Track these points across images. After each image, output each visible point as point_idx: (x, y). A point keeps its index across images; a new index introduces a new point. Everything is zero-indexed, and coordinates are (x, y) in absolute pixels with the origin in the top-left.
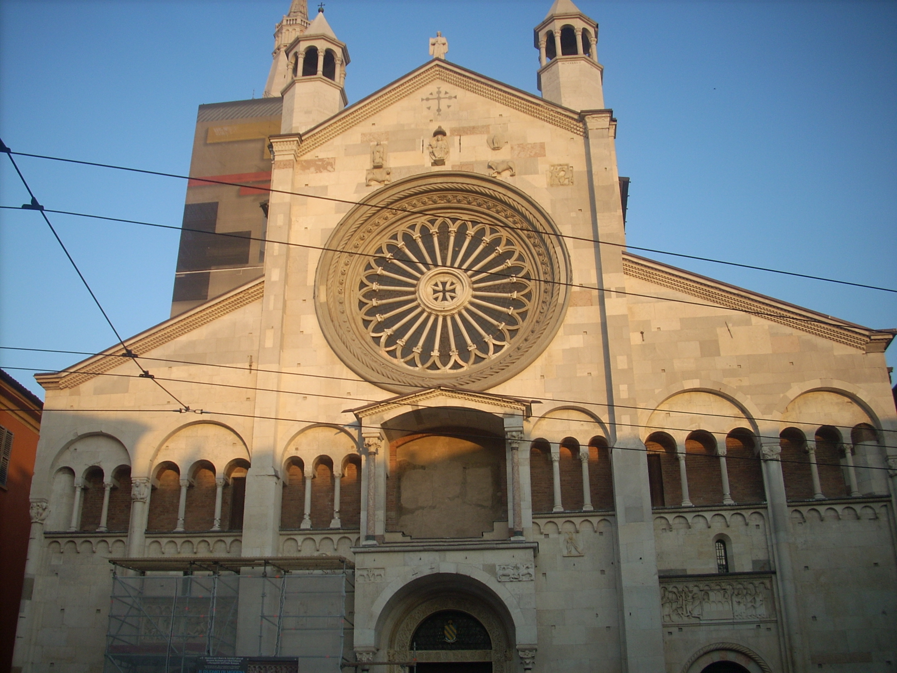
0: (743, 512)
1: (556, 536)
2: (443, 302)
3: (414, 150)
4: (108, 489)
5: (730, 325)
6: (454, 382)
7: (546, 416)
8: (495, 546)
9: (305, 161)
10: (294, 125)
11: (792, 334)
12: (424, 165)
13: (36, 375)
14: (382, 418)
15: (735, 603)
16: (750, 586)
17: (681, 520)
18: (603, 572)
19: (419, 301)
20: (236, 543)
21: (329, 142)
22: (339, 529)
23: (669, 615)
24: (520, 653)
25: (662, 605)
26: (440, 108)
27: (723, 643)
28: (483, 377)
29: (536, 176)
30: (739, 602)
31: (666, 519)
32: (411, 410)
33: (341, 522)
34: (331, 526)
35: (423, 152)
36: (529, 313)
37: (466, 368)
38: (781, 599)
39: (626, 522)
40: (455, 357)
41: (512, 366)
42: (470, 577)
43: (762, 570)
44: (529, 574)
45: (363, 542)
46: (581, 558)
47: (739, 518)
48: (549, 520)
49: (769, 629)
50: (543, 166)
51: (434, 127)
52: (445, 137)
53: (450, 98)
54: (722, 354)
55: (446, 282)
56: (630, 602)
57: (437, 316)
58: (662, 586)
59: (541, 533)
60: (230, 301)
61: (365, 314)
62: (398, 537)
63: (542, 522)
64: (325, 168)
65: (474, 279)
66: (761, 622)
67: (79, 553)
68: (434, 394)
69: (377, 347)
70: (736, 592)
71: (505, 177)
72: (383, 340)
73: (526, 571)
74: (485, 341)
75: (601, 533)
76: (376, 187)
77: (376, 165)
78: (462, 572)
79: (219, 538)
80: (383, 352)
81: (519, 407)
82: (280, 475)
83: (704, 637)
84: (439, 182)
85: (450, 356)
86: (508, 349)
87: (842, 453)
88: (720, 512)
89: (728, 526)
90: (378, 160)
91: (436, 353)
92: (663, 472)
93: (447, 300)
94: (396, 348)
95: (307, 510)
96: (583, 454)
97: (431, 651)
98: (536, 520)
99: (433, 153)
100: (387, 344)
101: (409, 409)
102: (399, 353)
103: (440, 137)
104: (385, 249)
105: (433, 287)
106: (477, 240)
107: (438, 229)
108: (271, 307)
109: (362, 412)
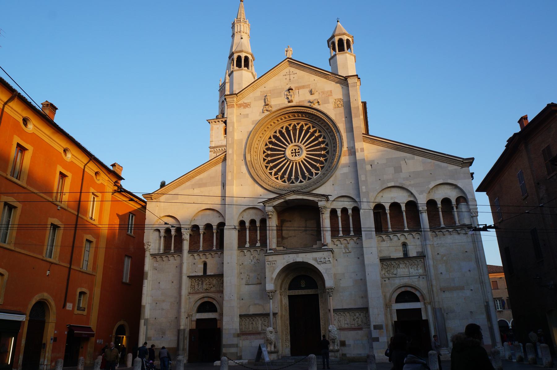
0: (412, 233)
1: (340, 245)
3: (281, 97)
4: (173, 236)
5: (406, 160)
7: (335, 200)
8: (316, 250)
9: (239, 104)
10: (234, 90)
11: (431, 162)
13: (143, 195)
14: (273, 205)
15: (409, 268)
16: (416, 262)
17: (388, 237)
18: (358, 258)
19: (286, 157)
20: (222, 254)
21: (248, 96)
22: (259, 246)
23: (384, 274)
24: (327, 290)
25: (382, 270)
26: (291, 78)
27: (405, 284)
29: (328, 104)
30: (411, 268)
31: (382, 237)
33: (261, 244)
34: (257, 245)
36: (328, 159)
37: (305, 182)
38: (428, 266)
39: (366, 239)
41: (321, 181)
42: (307, 263)
43: (421, 255)
44: (329, 260)
45: (268, 252)
46: (350, 253)
47: (411, 236)
48: (338, 239)
49: (423, 278)
50: (332, 100)
51: (288, 88)
52: (293, 91)
53: (294, 74)
54: (403, 172)
55: (296, 149)
56: (368, 270)
57: (293, 163)
58: (381, 263)
59: (335, 245)
61: (266, 163)
62: (282, 248)
63: (335, 240)
64: (247, 107)
65: (307, 147)
66: (420, 275)
67: (164, 261)
68: (292, 194)
70: (410, 264)
71: (316, 106)
72: (273, 173)
73: (328, 260)
75: (357, 243)
76: (267, 113)
77: (266, 104)
79: (216, 252)
80: (273, 178)
81: (324, 197)
82: (237, 227)
83: (398, 282)
86: (320, 174)
87: (453, 208)
88: (403, 234)
89: (407, 239)
91: (293, 177)
92: (381, 219)
93: (296, 156)
95: (248, 240)
96: (349, 214)
97: (295, 291)
98: (332, 240)
99: (288, 98)
100: (274, 175)
101: (283, 200)
102: (279, 178)
103: (291, 91)
104: (272, 137)
106: (307, 131)
108: (230, 164)
109: (265, 203)
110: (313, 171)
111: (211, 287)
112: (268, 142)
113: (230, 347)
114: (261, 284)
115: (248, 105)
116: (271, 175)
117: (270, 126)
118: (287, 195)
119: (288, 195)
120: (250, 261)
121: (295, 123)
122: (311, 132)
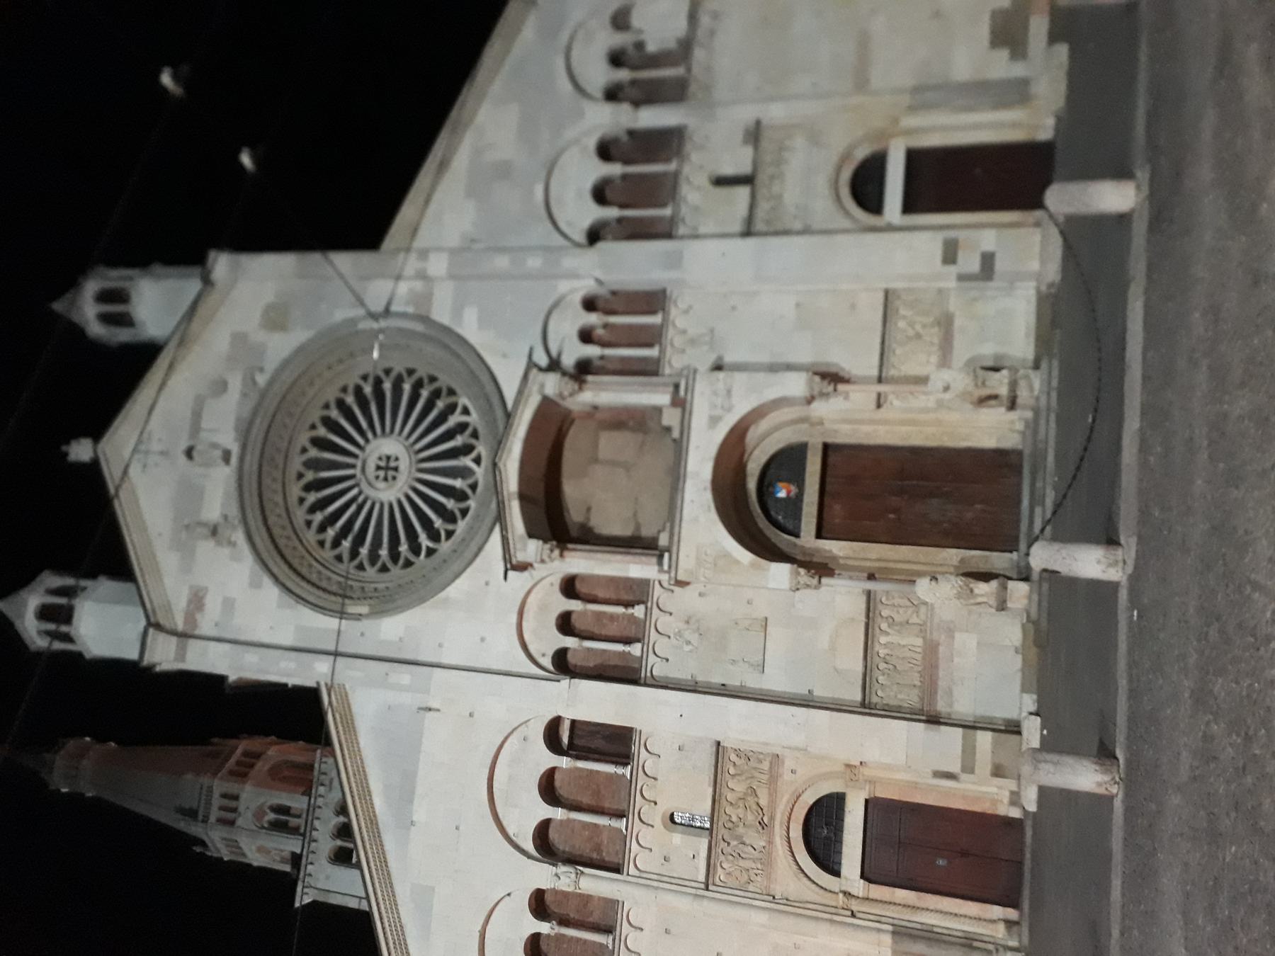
22: (646, 608)
37: (482, 449)
40: (467, 461)
50: (259, 336)
51: (182, 459)
60: (341, 732)
71: (262, 380)
72: (431, 545)
76: (239, 536)
78: (713, 450)
86: (469, 398)
90: (205, 531)
91: (458, 483)
102: (450, 527)
103: (195, 454)
104: (321, 537)
110: (453, 420)
111: (758, 804)
113: (974, 747)
114: (766, 619)
115: (196, 595)
120: (687, 648)
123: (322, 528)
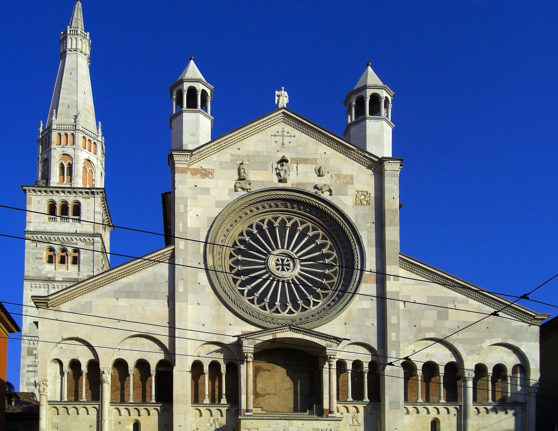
2: (282, 272)
6: (290, 322)
12: (273, 182)
28: (311, 321)
32: (272, 338)
35: (272, 173)
37: (296, 314)
40: (290, 307)
62: (259, 410)
64: (208, 176)
68: (286, 330)
69: (242, 296)
72: (246, 292)
74: (308, 298)
76: (242, 193)
77: (242, 177)
80: (246, 300)
84: (283, 194)
85: (286, 306)
91: (278, 303)
93: (284, 270)
94: (254, 298)
102: (255, 301)
104: (245, 234)
105: (276, 261)
106: (303, 234)
107: (279, 224)
112: (238, 240)
116: (243, 294)
117: (243, 215)
118: (279, 330)
119: (281, 330)
121: (284, 217)
122: (309, 237)
123: (249, 233)
